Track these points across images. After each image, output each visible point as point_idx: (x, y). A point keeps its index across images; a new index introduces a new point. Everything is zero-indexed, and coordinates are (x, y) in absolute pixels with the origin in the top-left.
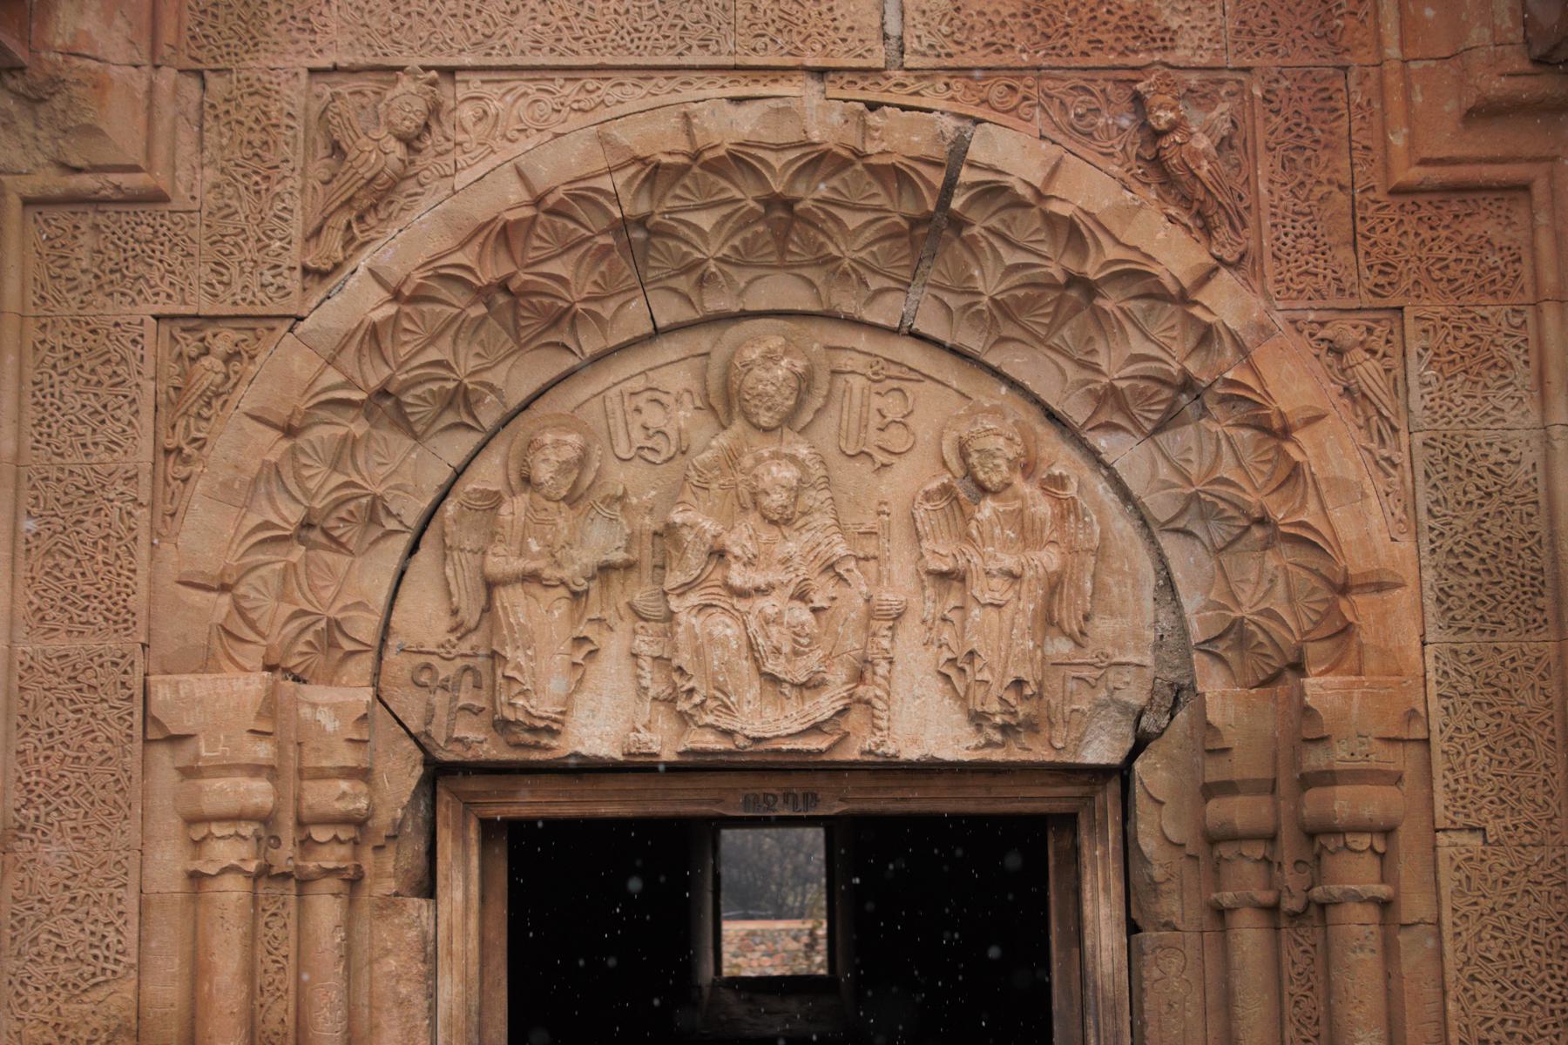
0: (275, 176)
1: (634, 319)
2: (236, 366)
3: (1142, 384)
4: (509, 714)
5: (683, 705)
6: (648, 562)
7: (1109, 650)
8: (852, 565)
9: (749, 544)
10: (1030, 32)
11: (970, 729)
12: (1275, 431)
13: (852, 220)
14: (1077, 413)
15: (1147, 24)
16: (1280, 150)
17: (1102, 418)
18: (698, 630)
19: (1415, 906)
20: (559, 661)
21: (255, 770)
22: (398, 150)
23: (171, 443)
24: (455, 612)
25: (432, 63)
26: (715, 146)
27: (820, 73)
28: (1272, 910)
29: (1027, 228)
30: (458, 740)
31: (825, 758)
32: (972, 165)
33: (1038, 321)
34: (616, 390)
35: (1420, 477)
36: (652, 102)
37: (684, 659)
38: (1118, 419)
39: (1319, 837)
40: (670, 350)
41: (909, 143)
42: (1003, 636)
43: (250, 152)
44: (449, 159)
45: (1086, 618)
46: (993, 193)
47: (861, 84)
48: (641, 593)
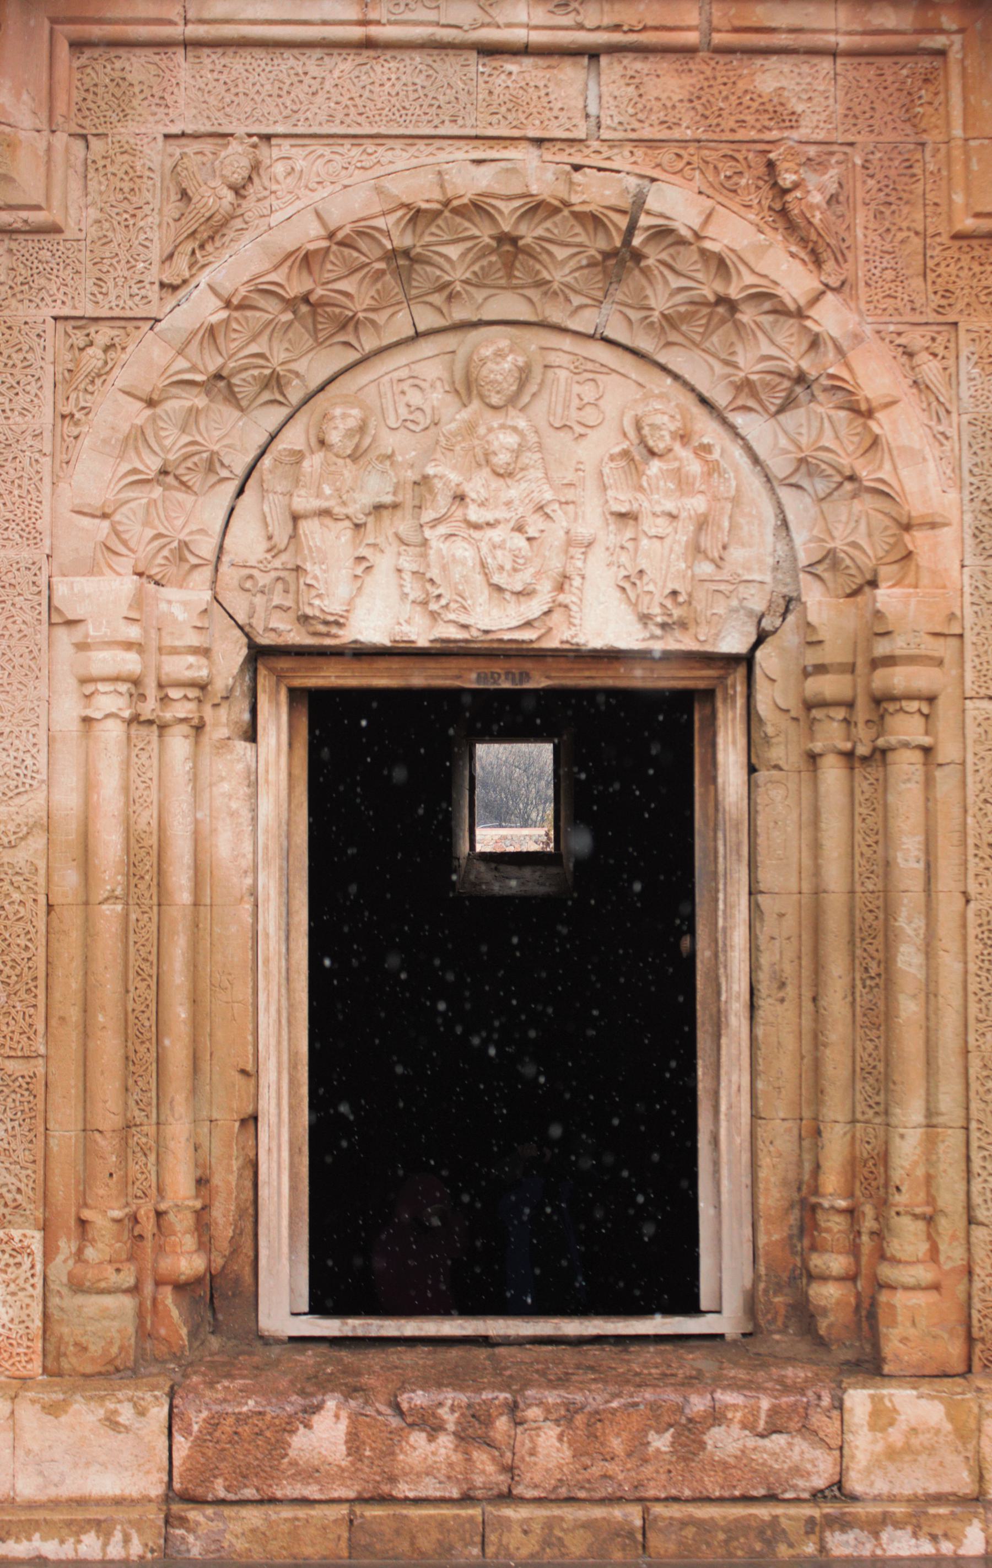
0: (140, 214)
1: (400, 326)
2: (112, 354)
3: (768, 377)
4: (309, 611)
5: (434, 606)
6: (409, 503)
7: (740, 571)
8: (556, 506)
10: (692, 113)
11: (639, 626)
12: (863, 412)
13: (561, 253)
14: (721, 397)
15: (779, 109)
16: (873, 206)
17: (740, 402)
19: (948, 751)
20: (345, 574)
21: (129, 645)
22: (229, 196)
23: (66, 411)
24: (270, 538)
25: (253, 131)
27: (539, 142)
28: (849, 755)
29: (688, 260)
30: (273, 630)
31: (535, 646)
32: (648, 213)
33: (694, 330)
34: (387, 378)
35: (965, 446)
36: (415, 162)
37: (434, 573)
38: (751, 403)
39: (882, 702)
40: (427, 348)
42: (664, 559)
43: (121, 197)
44: (266, 203)
45: (724, 548)
46: (663, 233)
47: (568, 151)
48: (403, 525)
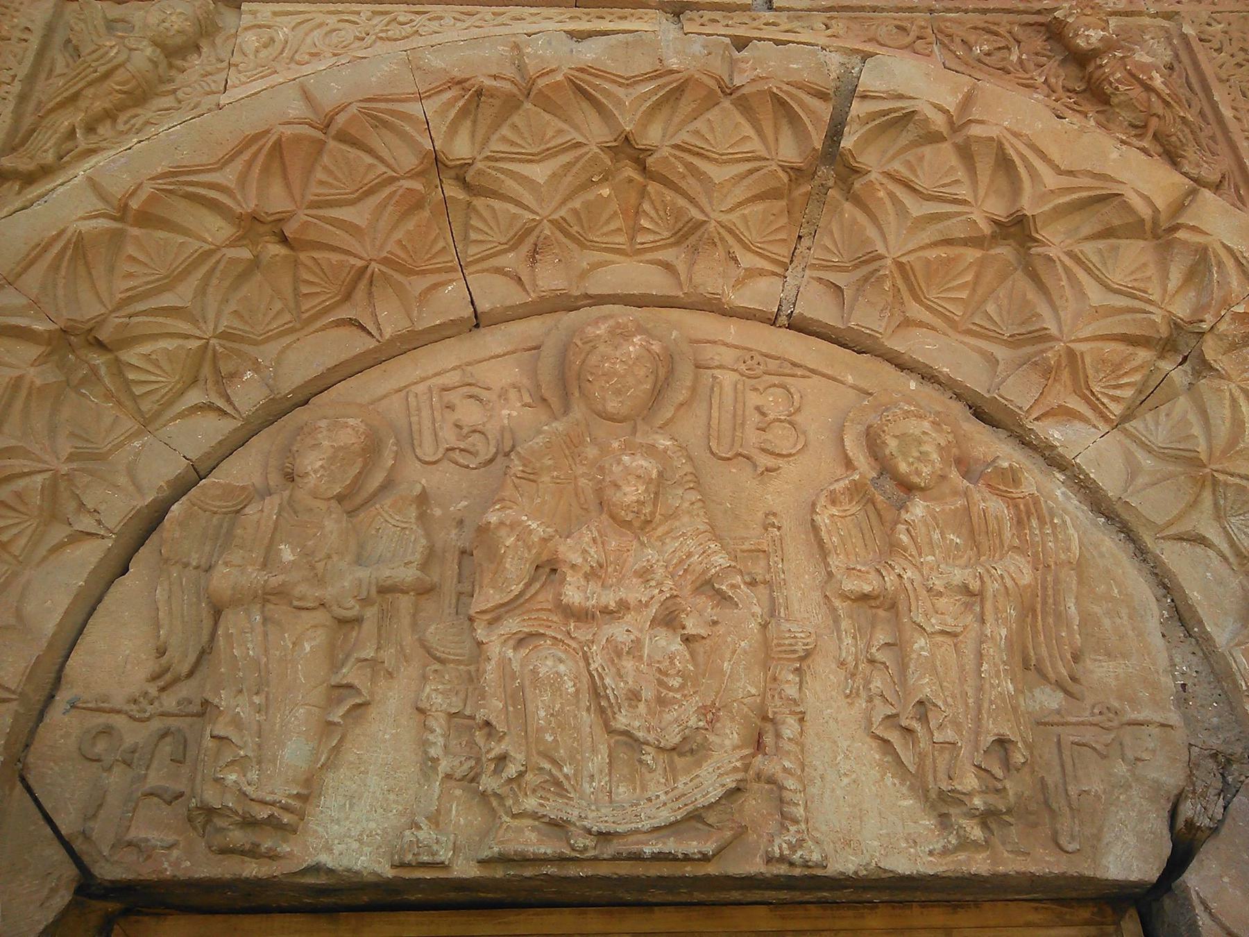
3: (1109, 347)
4: (211, 796)
5: (488, 782)
6: (450, 586)
9: (592, 551)
11: (928, 822)
17: (1052, 401)
18: (516, 666)
24: (161, 652)
26: (552, 71)
31: (711, 869)
34: (421, 388)
37: (493, 708)
38: (1075, 403)
40: (494, 340)
41: (787, 69)
45: (1076, 658)
